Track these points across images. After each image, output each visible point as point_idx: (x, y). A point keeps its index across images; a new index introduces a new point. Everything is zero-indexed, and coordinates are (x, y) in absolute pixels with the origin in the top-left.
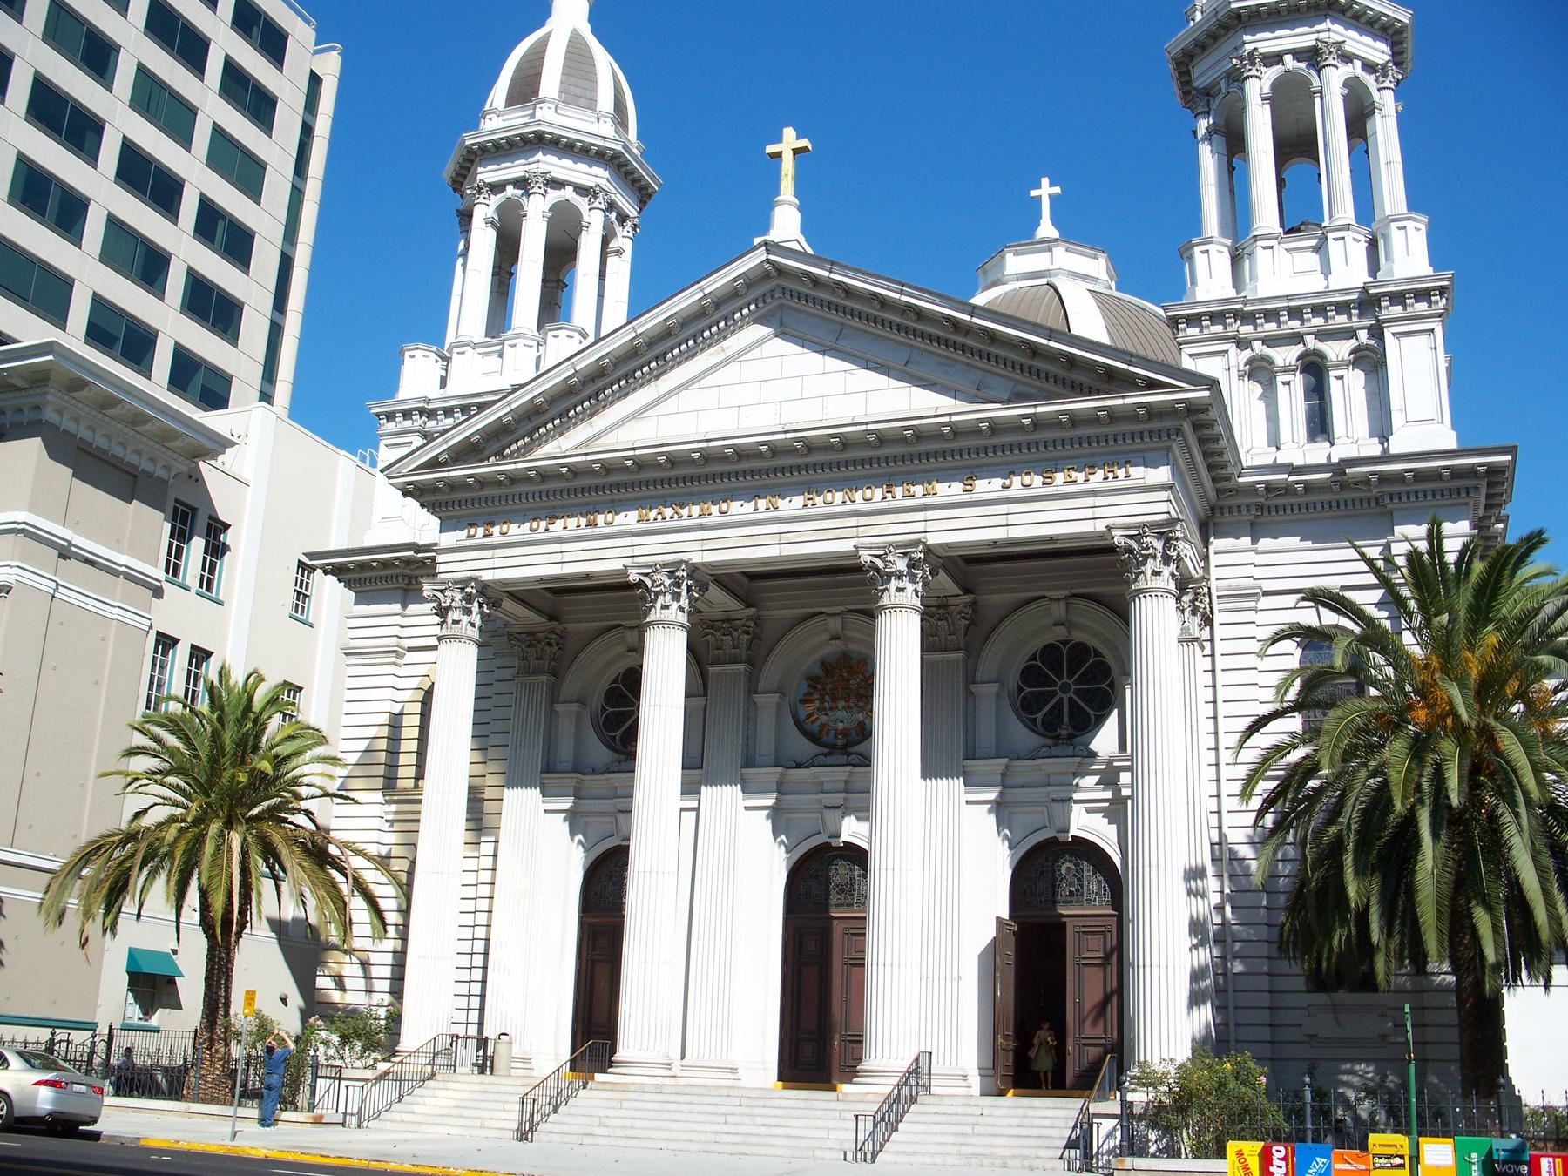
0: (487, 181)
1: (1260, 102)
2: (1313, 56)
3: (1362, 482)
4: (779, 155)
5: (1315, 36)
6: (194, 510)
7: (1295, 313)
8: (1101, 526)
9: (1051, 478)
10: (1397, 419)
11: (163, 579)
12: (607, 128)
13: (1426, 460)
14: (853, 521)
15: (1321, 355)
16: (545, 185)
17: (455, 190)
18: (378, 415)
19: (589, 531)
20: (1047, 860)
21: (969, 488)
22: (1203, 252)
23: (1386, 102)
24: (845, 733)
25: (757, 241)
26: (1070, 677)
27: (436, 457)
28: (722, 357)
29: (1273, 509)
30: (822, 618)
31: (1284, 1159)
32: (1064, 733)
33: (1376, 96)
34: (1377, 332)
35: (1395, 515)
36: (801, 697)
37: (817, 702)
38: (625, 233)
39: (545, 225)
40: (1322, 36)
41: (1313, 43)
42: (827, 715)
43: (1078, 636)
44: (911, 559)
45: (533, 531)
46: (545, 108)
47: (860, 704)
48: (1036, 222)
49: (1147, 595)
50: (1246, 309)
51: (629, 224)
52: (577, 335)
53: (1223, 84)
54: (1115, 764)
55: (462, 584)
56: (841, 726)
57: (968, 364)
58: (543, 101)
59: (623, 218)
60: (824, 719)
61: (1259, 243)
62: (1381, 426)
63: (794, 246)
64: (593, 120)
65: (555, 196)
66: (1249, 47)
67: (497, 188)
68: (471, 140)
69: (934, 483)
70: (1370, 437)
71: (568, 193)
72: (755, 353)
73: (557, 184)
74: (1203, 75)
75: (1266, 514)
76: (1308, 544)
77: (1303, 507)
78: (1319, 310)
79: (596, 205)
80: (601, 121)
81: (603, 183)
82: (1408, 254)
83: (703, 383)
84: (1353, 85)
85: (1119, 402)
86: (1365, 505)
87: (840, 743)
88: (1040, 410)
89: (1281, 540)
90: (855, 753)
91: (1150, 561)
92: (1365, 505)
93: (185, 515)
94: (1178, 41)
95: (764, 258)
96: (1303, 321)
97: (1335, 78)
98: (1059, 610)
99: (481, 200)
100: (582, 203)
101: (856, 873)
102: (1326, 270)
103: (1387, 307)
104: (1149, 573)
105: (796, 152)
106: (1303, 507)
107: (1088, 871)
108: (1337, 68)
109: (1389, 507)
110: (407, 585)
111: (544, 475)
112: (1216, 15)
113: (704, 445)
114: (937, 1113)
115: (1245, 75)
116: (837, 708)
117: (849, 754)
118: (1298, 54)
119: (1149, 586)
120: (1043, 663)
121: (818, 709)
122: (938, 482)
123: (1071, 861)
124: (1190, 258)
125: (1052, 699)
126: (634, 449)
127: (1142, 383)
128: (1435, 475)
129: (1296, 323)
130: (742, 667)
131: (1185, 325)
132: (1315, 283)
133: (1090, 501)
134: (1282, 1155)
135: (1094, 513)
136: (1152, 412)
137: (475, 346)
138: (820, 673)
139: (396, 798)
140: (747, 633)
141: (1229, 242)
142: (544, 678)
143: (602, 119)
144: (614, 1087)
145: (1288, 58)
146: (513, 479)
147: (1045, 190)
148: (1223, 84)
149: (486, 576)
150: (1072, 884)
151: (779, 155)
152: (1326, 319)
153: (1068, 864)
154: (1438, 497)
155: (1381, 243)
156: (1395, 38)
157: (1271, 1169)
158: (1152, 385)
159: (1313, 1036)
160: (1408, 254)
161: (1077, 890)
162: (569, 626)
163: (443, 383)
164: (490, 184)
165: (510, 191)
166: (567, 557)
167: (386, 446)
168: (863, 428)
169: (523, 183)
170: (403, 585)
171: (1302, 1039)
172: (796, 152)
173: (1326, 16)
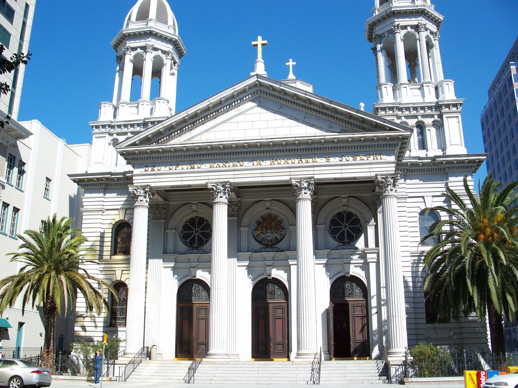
0: (130, 46)
1: (400, 41)
2: (417, 28)
3: (440, 163)
4: (257, 45)
5: (417, 22)
6: (14, 157)
7: (415, 109)
8: (373, 174)
9: (356, 158)
10: (448, 144)
11: (6, 182)
12: (172, 31)
13: (461, 157)
14: (288, 170)
15: (423, 122)
16: (152, 49)
17: (114, 49)
18: (92, 126)
19: (192, 170)
20: (341, 283)
21: (328, 160)
22: (385, 87)
23: (436, 43)
24: (271, 240)
25: (252, 74)
26: (347, 223)
27: (135, 142)
28: (238, 112)
29: (411, 171)
30: (263, 202)
31: (485, 376)
32: (346, 241)
33: (433, 42)
34: (441, 116)
35: (449, 173)
36: (254, 228)
37: (261, 230)
38: (175, 68)
40: (420, 22)
41: (417, 24)
42: (264, 234)
43: (350, 210)
44: (309, 183)
45: (146, 171)
46: (152, 23)
47: (276, 231)
48: (288, 74)
49: (389, 197)
50: (400, 106)
51: (176, 65)
52: (166, 102)
53: (386, 34)
54: (366, 251)
55: (144, 188)
56: (269, 238)
57: (326, 120)
58: (151, 20)
59: (175, 63)
60: (263, 236)
61: (402, 86)
62: (442, 146)
63: (265, 76)
64: (167, 28)
65: (155, 53)
66: (397, 23)
67: (134, 49)
68: (125, 30)
69: (316, 158)
70: (438, 149)
71: (159, 53)
72: (250, 112)
73: (156, 49)
74: (379, 30)
75: (409, 172)
76: (422, 182)
77: (420, 170)
78: (423, 108)
79: (169, 57)
80: (170, 29)
81: (171, 50)
82: (449, 92)
83: (231, 121)
84: (427, 37)
85: (381, 134)
86: (440, 170)
87: (270, 244)
88: (355, 136)
89: (413, 180)
90: (275, 248)
91: (389, 186)
92: (440, 170)
93: (11, 159)
94: (370, 20)
95: (256, 79)
96: (417, 111)
97: (424, 35)
98: (345, 201)
99: (128, 53)
100: (164, 56)
101: (276, 287)
102: (423, 96)
103: (444, 109)
104: (389, 190)
105: (262, 45)
106: (420, 170)
107: (355, 286)
108: (424, 32)
109: (447, 171)
110: (106, 187)
111: (176, 150)
112: (386, 12)
113: (237, 142)
114: (329, 367)
115: (396, 32)
116: (268, 232)
117: (273, 248)
118: (412, 27)
119: (389, 194)
120: (337, 218)
121: (261, 232)
122: (317, 158)
123: (349, 283)
124: (380, 89)
125: (341, 230)
126: (211, 142)
127: (388, 129)
128: (463, 162)
129: (415, 112)
130: (236, 218)
131: (380, 111)
132: (419, 100)
133: (369, 166)
134: (484, 374)
135: (370, 170)
136: (392, 138)
137: (127, 104)
138: (261, 220)
139: (103, 262)
140: (237, 206)
141: (392, 85)
142: (163, 221)
143: (170, 28)
144: (211, 363)
145: (409, 28)
146: (164, 151)
147: (291, 63)
148: (386, 34)
149: (152, 185)
150: (350, 290)
151: (257, 45)
152: (425, 111)
153: (348, 284)
154: (463, 169)
155: (440, 89)
156: (438, 25)
157: (481, 379)
158: (391, 130)
159: (428, 338)
160: (449, 92)
161: (352, 292)
162: (171, 203)
163: (115, 116)
164: (131, 47)
165: (139, 50)
166: (183, 179)
167: (95, 137)
168: (294, 139)
169: (144, 48)
170: (104, 187)
171: (425, 338)
172: (262, 45)
173: (420, 16)
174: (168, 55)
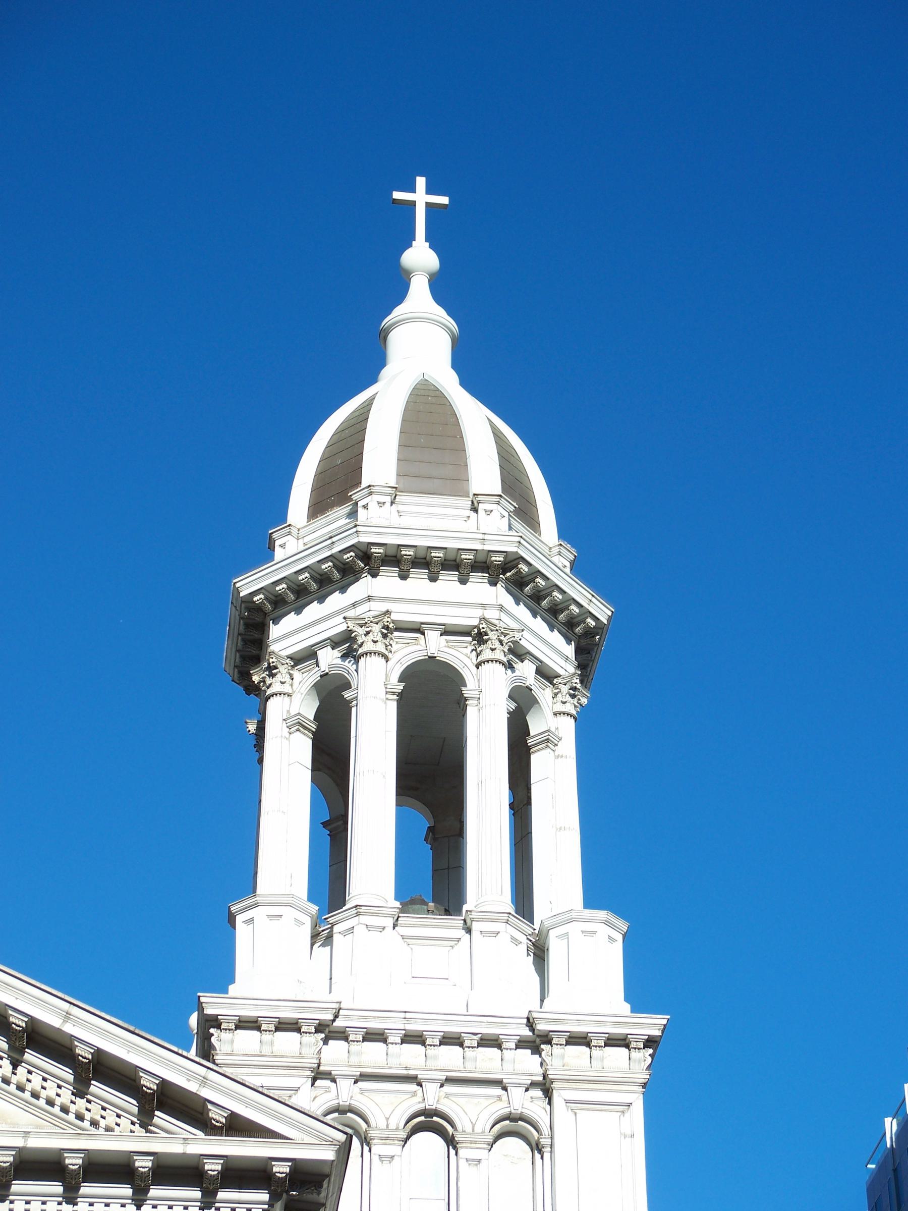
38: (559, 707)
39: (393, 707)
46: (373, 506)
59: (546, 674)
79: (487, 654)
143: (481, 507)
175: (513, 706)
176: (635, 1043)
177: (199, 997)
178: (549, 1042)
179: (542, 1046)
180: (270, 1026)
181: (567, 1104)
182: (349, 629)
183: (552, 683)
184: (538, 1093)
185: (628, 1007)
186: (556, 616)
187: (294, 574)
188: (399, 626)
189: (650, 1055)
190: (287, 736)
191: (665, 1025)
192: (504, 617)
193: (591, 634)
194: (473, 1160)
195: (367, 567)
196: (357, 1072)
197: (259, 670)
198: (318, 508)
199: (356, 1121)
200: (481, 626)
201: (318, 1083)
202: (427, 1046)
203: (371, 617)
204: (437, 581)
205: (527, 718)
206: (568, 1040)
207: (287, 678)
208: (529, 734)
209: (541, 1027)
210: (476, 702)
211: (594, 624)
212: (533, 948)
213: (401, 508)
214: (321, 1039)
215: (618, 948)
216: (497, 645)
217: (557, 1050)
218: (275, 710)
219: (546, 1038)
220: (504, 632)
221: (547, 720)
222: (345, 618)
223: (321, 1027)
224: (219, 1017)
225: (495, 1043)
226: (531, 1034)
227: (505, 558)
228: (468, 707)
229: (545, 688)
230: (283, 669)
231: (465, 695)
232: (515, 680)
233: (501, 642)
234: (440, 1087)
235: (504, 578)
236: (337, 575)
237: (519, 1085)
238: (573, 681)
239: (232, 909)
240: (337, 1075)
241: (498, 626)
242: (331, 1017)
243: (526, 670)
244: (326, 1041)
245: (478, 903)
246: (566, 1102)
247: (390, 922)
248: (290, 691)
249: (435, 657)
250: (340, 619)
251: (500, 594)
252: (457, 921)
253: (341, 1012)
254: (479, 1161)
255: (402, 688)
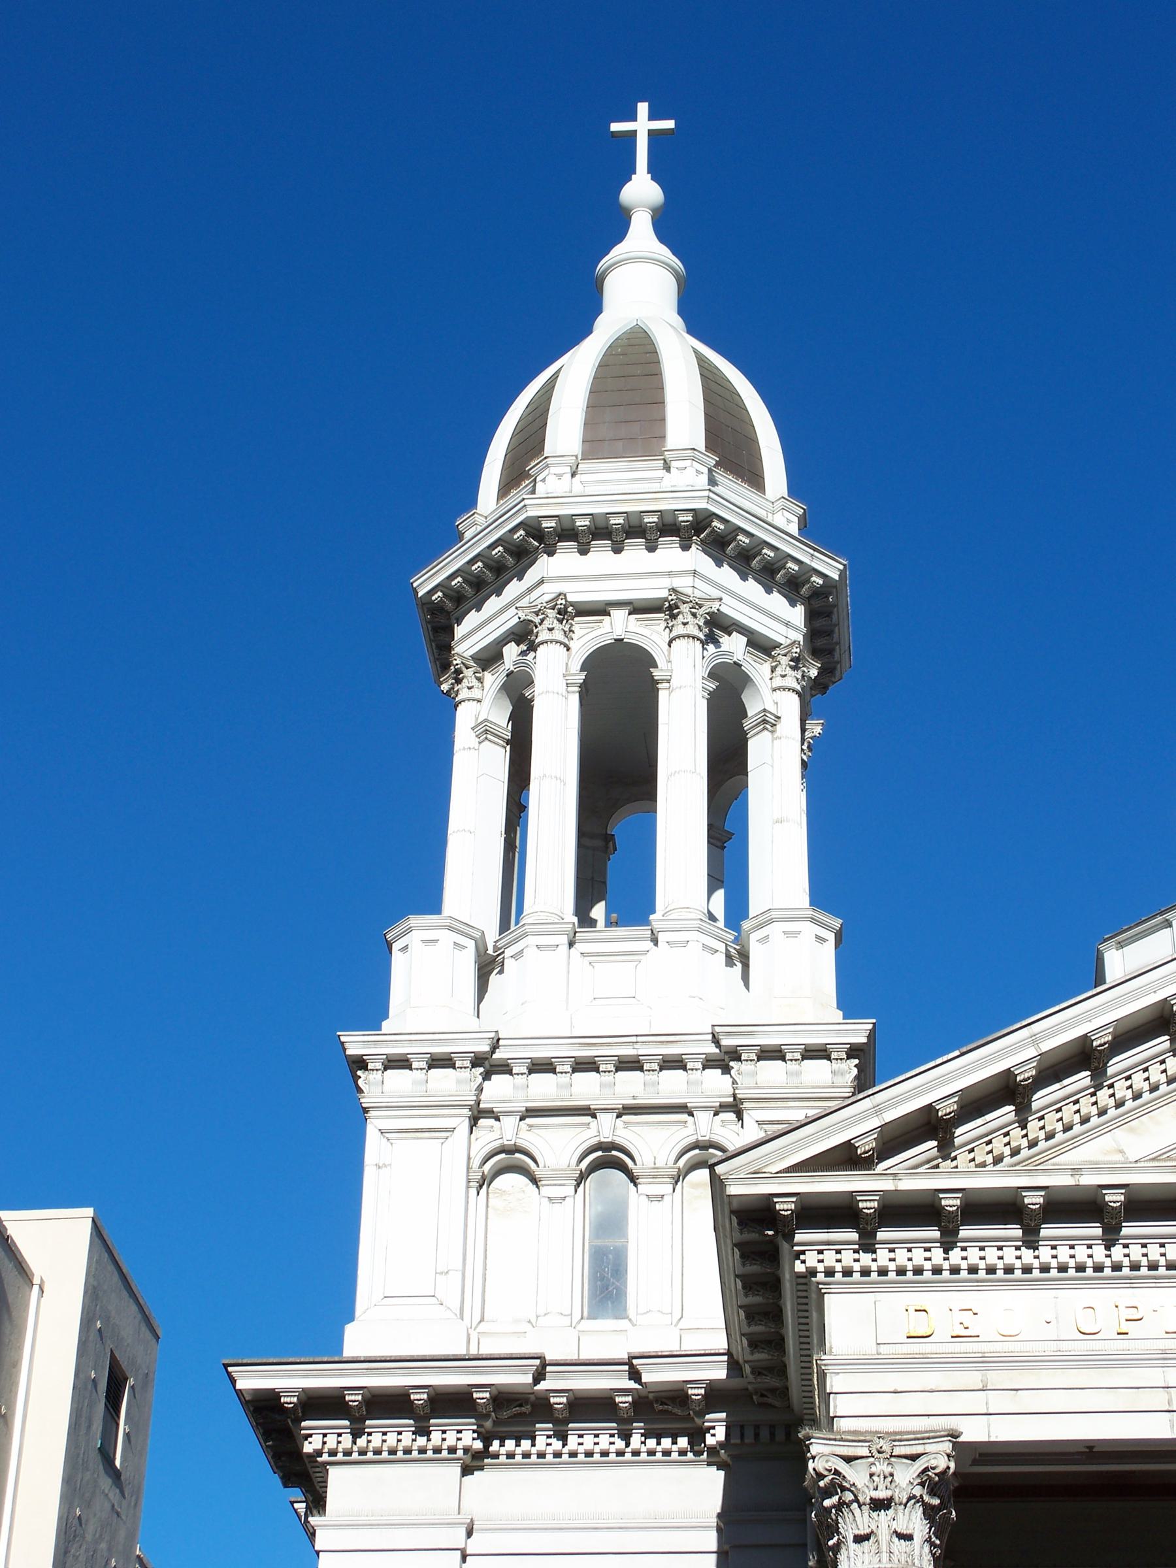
38: (778, 682)
39: (575, 700)
59: (761, 646)
73: (570, 612)
79: (679, 630)
143: (674, 464)
165: (511, 652)
169: (524, 635)
174: (673, 617)
175: (712, 686)
176: (791, 1054)
177: (339, 1036)
178: (738, 1059)
179: (732, 1064)
180: (465, 1062)
181: (760, 1126)
182: (521, 620)
183: (770, 655)
184: (732, 1116)
185: (841, 1013)
186: (773, 577)
187: (466, 565)
188: (582, 607)
189: (855, 1066)
190: (476, 747)
191: (870, 1030)
192: (698, 583)
193: (823, 594)
194: (656, 1196)
195: (542, 545)
196: (521, 1107)
197: (448, 677)
198: (505, 488)
199: (524, 1161)
200: (670, 598)
201: (482, 1122)
202: (558, 1074)
203: (543, 602)
204: (623, 552)
205: (742, 697)
206: (804, 1053)
207: (475, 683)
208: (746, 715)
209: (726, 1042)
210: (667, 685)
211: (821, 582)
212: (737, 956)
213: (584, 478)
214: (480, 1074)
215: (829, 949)
216: (690, 618)
217: (746, 1067)
218: (465, 718)
219: (735, 1054)
220: (699, 602)
221: (763, 696)
222: (516, 608)
223: (477, 1061)
224: (364, 1057)
225: (636, 1065)
226: (717, 1051)
227: (661, 517)
228: (660, 692)
229: (763, 662)
230: (468, 673)
231: (656, 678)
232: (715, 657)
233: (694, 615)
234: (714, 1115)
235: (699, 540)
236: (510, 560)
237: (705, 1108)
238: (793, 651)
239: (387, 937)
240: (500, 1113)
241: (692, 596)
242: (487, 1048)
243: (734, 646)
244: (487, 1076)
245: (667, 910)
246: (759, 1124)
247: (564, 940)
248: (480, 697)
249: (623, 639)
250: (513, 611)
251: (696, 558)
252: (645, 931)
253: (501, 1042)
254: (663, 1196)
255: (584, 677)
